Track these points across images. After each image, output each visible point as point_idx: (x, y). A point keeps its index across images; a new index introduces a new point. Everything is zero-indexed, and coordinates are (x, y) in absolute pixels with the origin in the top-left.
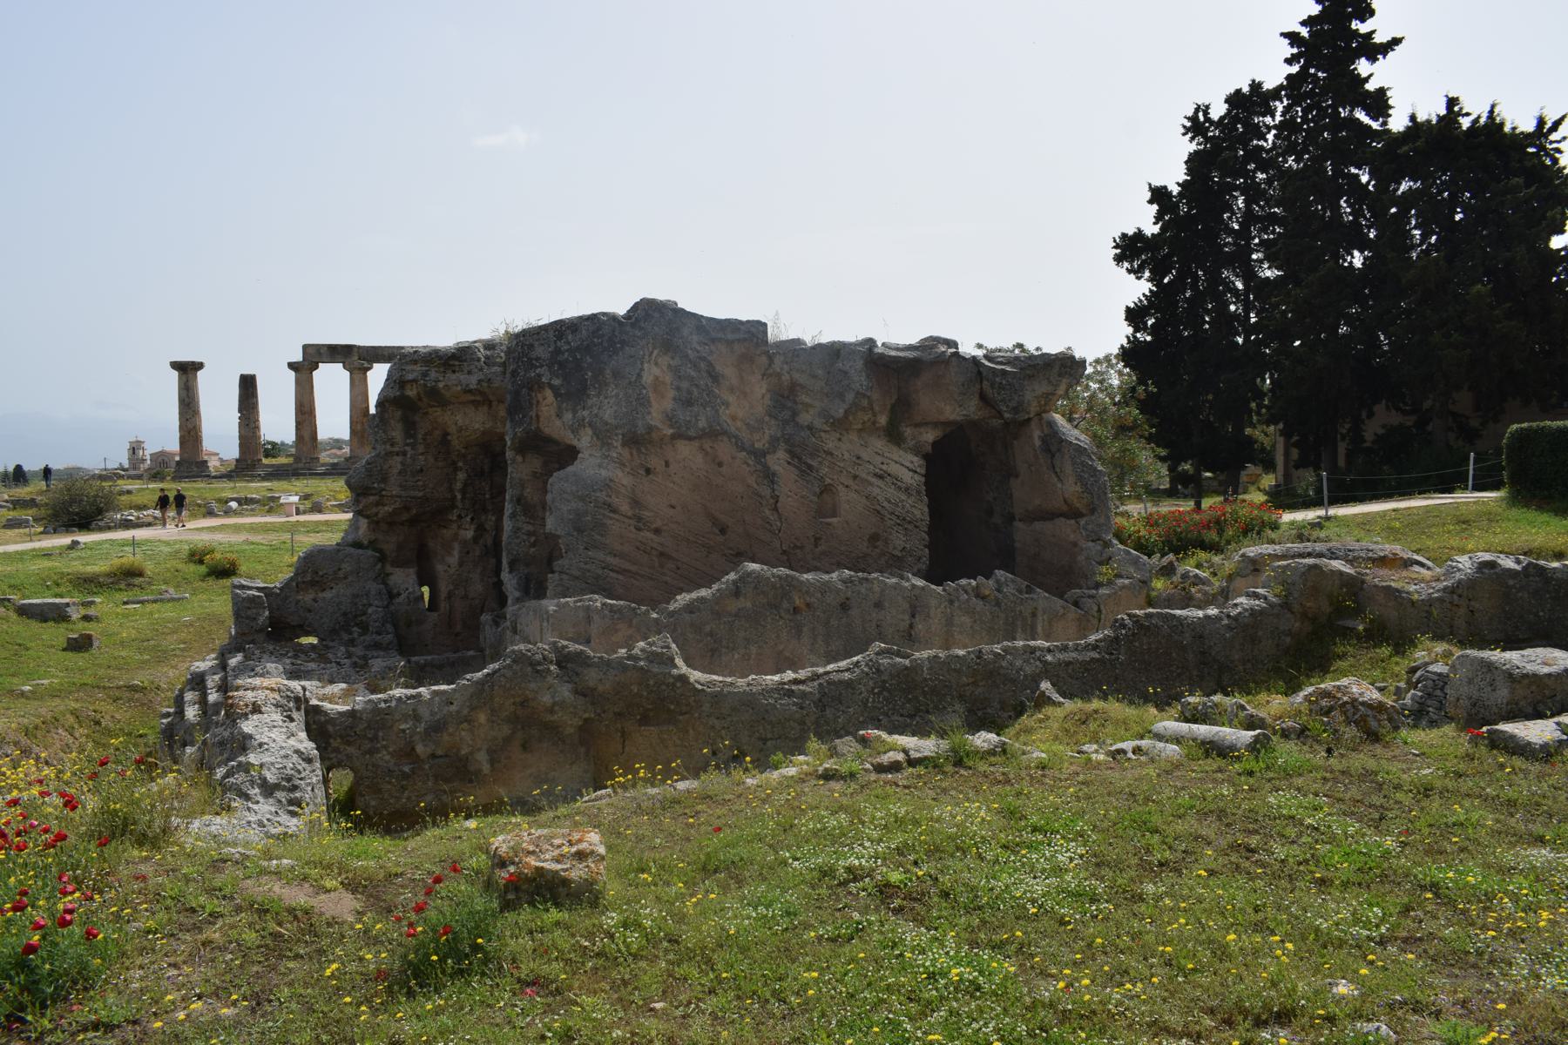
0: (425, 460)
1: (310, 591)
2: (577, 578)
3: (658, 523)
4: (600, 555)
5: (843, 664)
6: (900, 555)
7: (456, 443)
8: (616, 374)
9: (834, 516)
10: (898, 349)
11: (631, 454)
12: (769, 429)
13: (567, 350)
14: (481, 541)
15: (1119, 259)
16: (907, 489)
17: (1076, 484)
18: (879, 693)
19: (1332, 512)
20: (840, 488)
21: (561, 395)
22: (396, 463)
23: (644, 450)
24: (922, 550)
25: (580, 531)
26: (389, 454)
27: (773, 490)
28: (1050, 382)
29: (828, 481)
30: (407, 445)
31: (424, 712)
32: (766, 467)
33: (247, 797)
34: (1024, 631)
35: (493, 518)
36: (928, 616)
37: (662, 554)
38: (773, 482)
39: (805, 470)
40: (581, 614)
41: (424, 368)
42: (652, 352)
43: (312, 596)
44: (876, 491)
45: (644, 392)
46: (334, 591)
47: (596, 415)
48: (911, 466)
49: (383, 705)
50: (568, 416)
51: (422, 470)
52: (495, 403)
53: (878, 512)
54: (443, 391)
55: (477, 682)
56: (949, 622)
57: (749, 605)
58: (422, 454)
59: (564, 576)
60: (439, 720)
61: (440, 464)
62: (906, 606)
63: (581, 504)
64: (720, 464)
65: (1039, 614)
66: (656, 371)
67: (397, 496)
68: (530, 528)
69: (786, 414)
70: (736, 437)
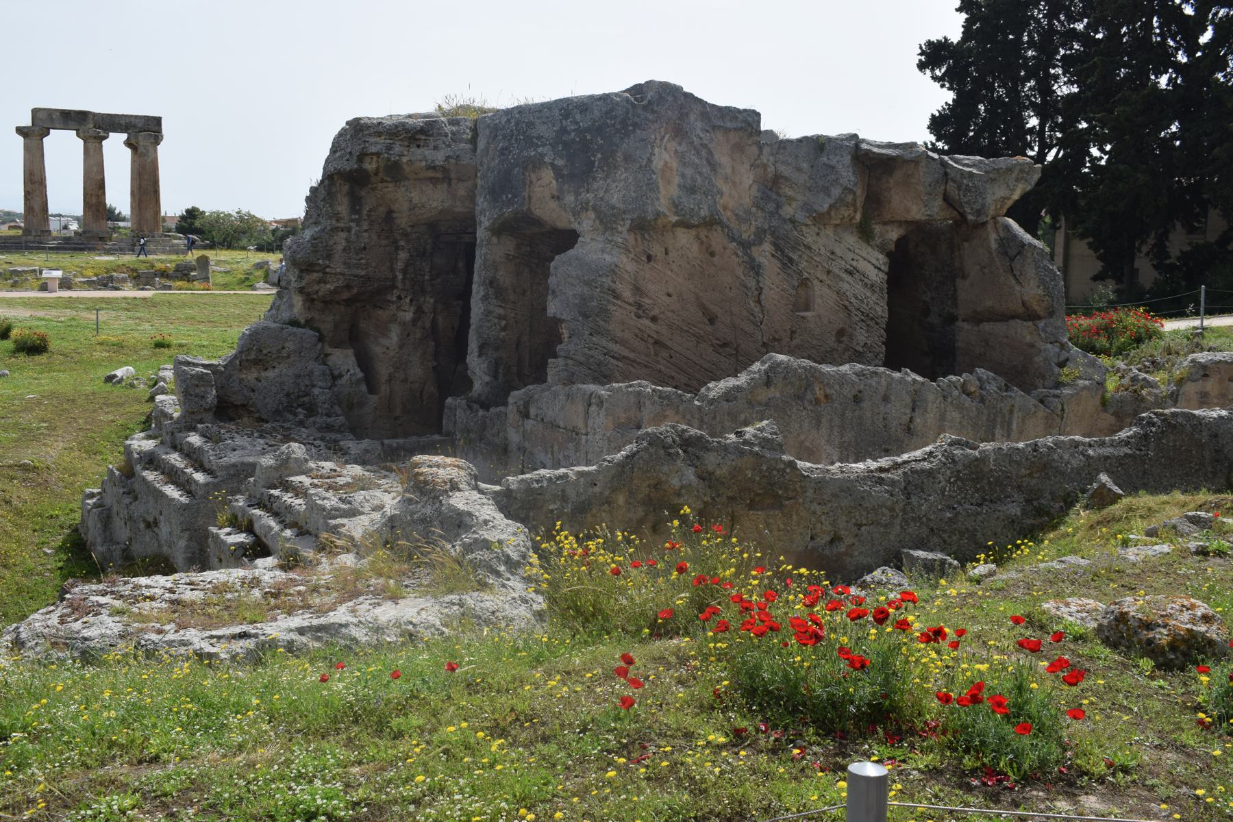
0: (370, 237)
1: (253, 369)
2: (581, 363)
3: (656, 312)
4: (603, 341)
5: (918, 453)
6: (861, 350)
7: (403, 221)
8: (628, 158)
9: (807, 309)
10: (879, 146)
11: (636, 240)
12: (756, 221)
13: (574, 131)
14: (419, 324)
15: (922, 66)
17: (1039, 287)
18: (955, 482)
19: (1206, 323)
20: (816, 282)
21: (562, 176)
22: (340, 240)
23: (647, 237)
24: (880, 347)
25: (585, 316)
26: (335, 230)
27: (758, 282)
28: (1008, 186)
30: (352, 221)
31: (571, 493)
32: (752, 259)
33: (498, 574)
34: (1002, 427)
35: (432, 301)
36: (926, 411)
37: (656, 342)
38: (758, 274)
39: (787, 263)
40: (632, 399)
41: (389, 141)
42: (664, 137)
43: (255, 375)
44: (846, 286)
45: (654, 177)
46: (276, 370)
47: (602, 199)
49: (535, 485)
50: (570, 198)
51: (365, 248)
52: (454, 182)
53: (846, 308)
54: (405, 166)
55: (618, 464)
56: (942, 417)
57: (778, 395)
58: (366, 231)
59: (570, 362)
60: (583, 502)
61: (384, 242)
62: (908, 400)
63: (586, 289)
64: (712, 254)
65: (1016, 411)
66: (666, 156)
67: (341, 274)
68: (501, 311)
69: (771, 207)
70: (728, 227)
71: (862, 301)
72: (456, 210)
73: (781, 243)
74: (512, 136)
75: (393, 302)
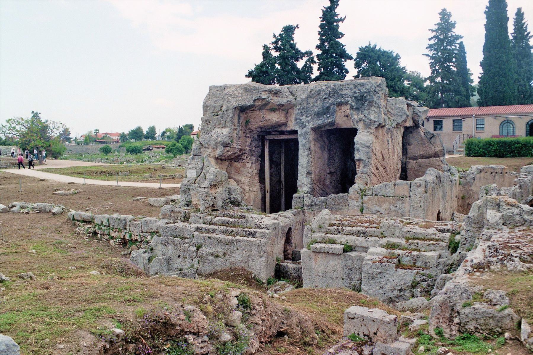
35: (254, 158)
46: (220, 189)
72: (281, 122)
74: (330, 93)
75: (244, 159)
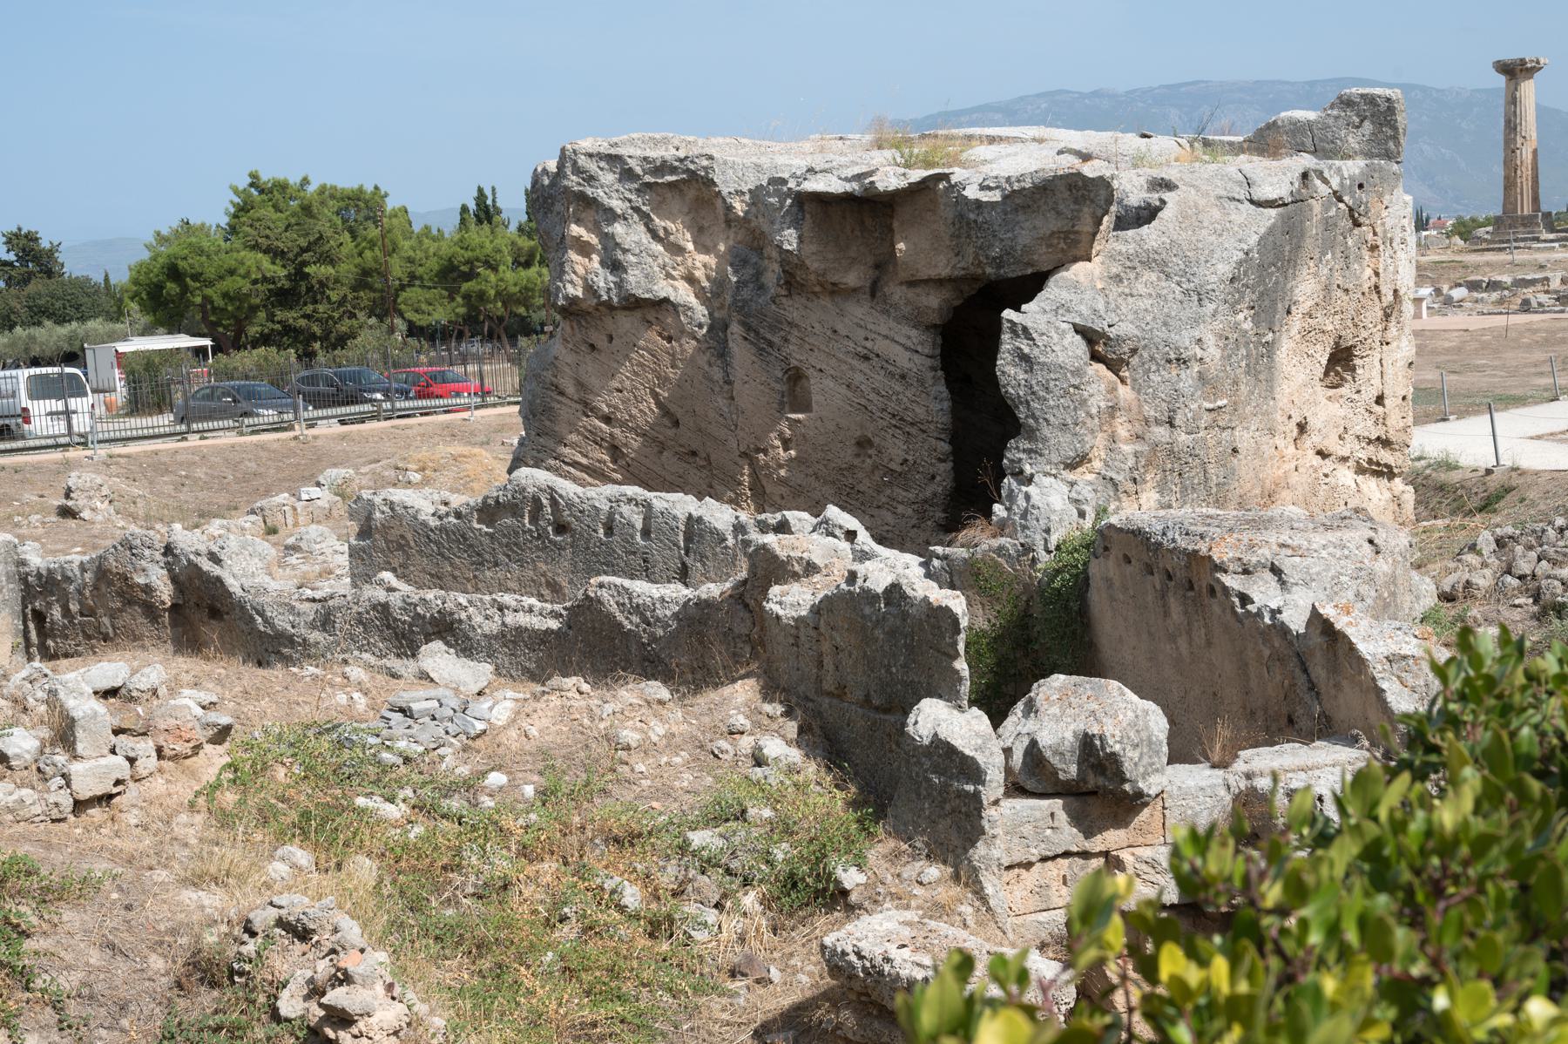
6: (899, 469)
11: (572, 328)
16: (903, 377)
29: (794, 363)
44: (858, 378)
48: (909, 344)
71: (889, 398)
73: (753, 322)
